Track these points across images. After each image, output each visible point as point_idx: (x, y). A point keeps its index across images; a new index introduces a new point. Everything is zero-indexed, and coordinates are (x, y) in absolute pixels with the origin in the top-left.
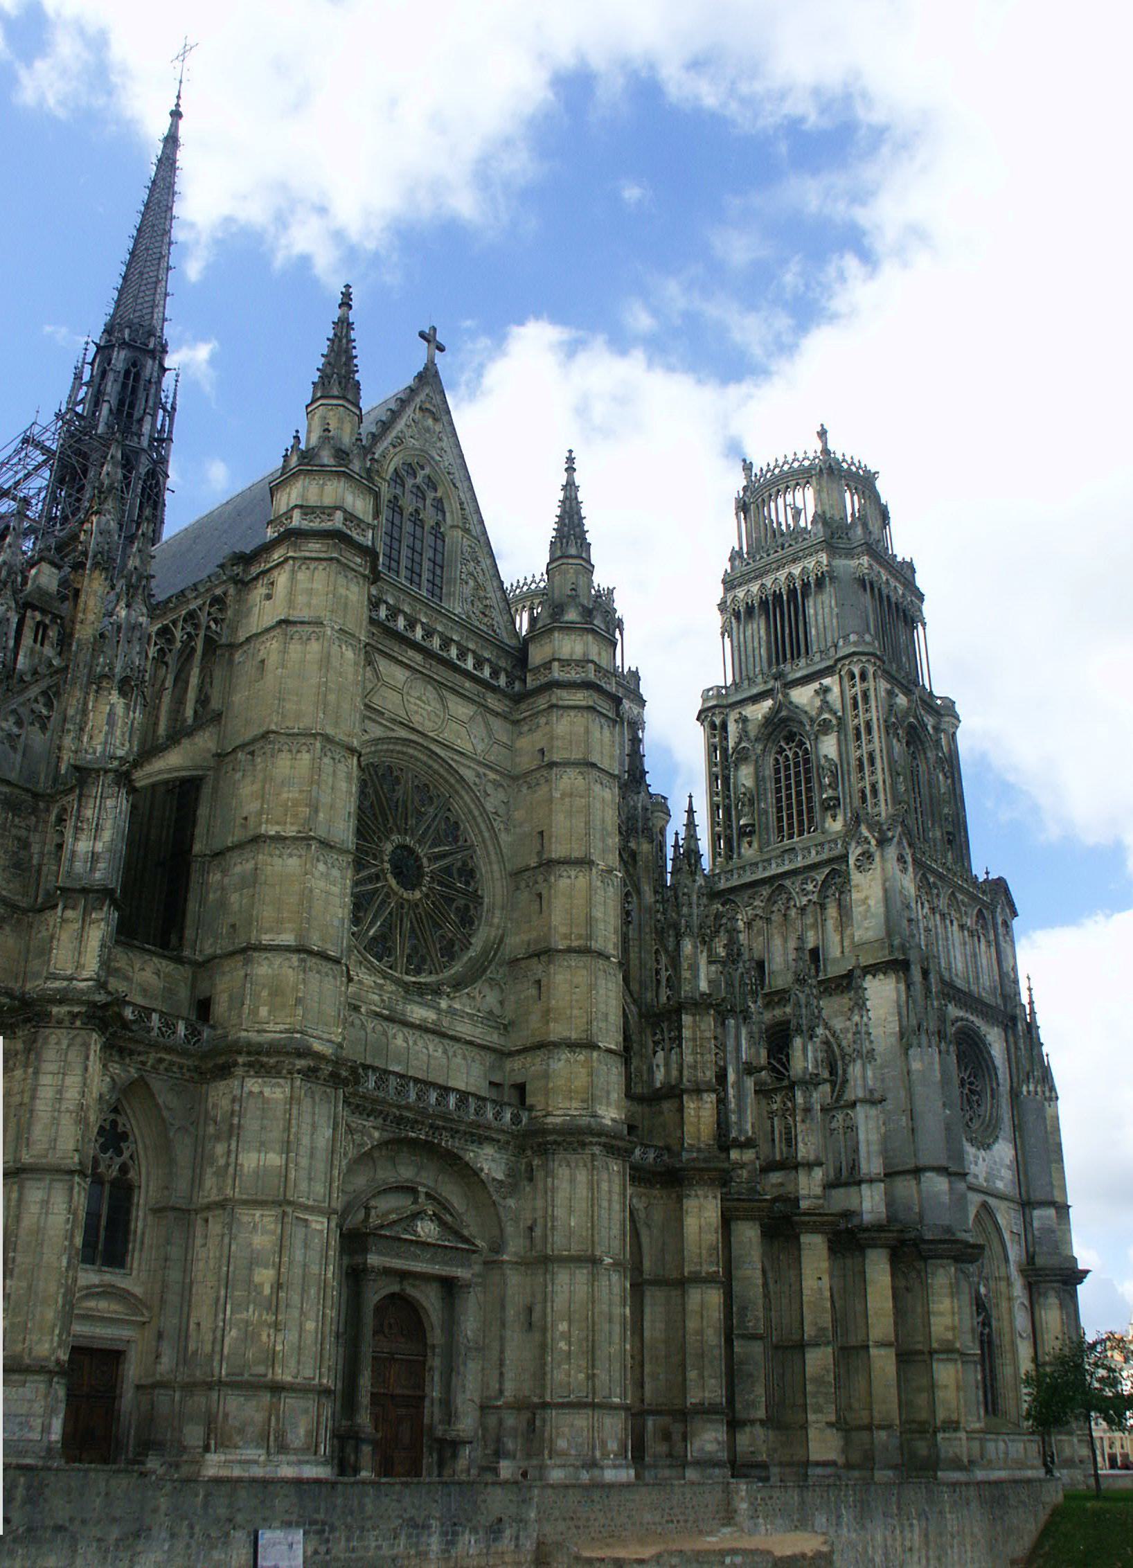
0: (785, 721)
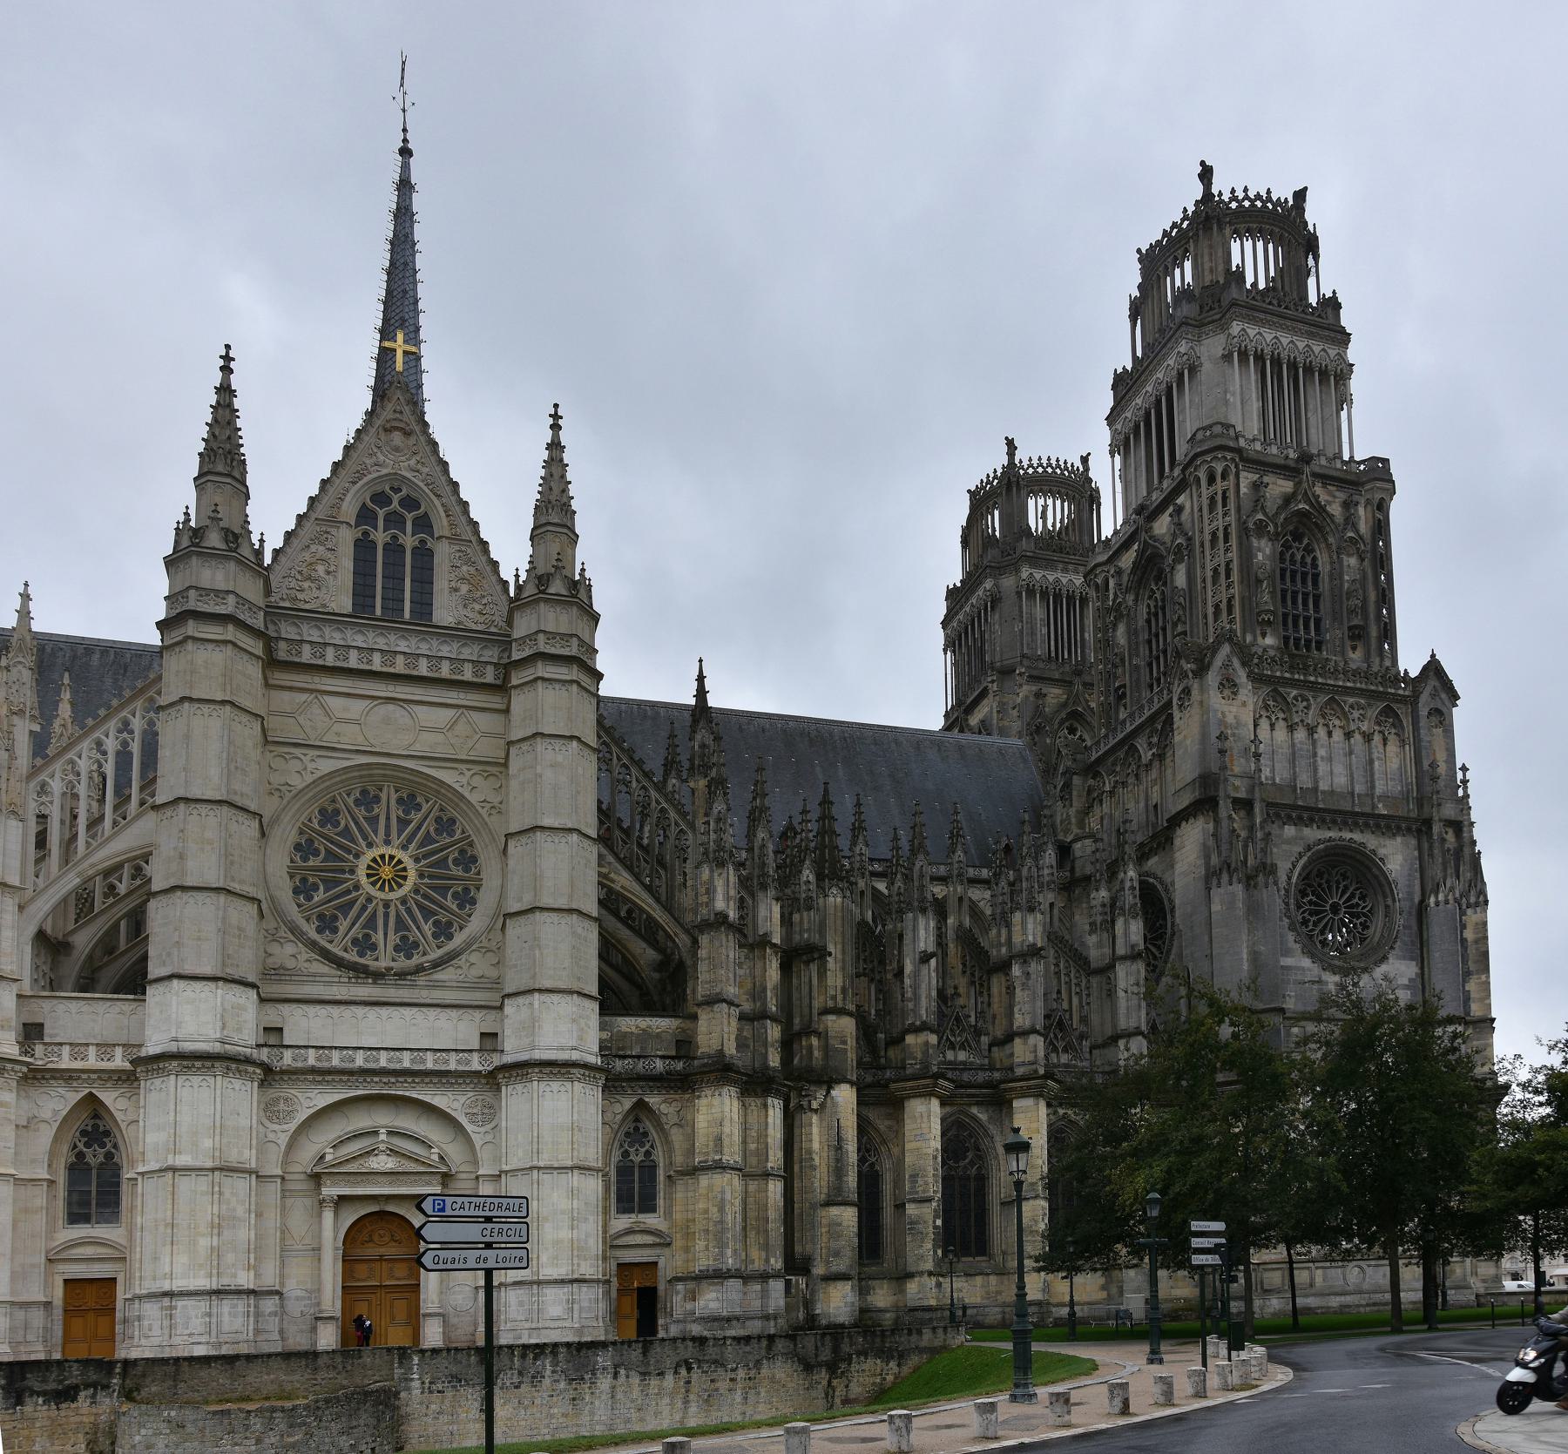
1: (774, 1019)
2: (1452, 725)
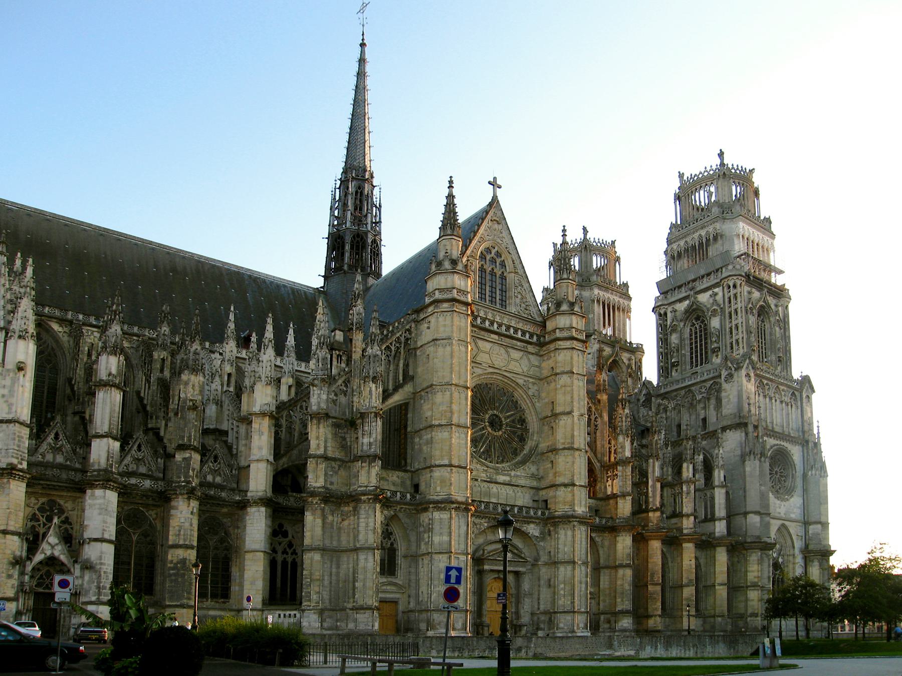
0: (694, 310)
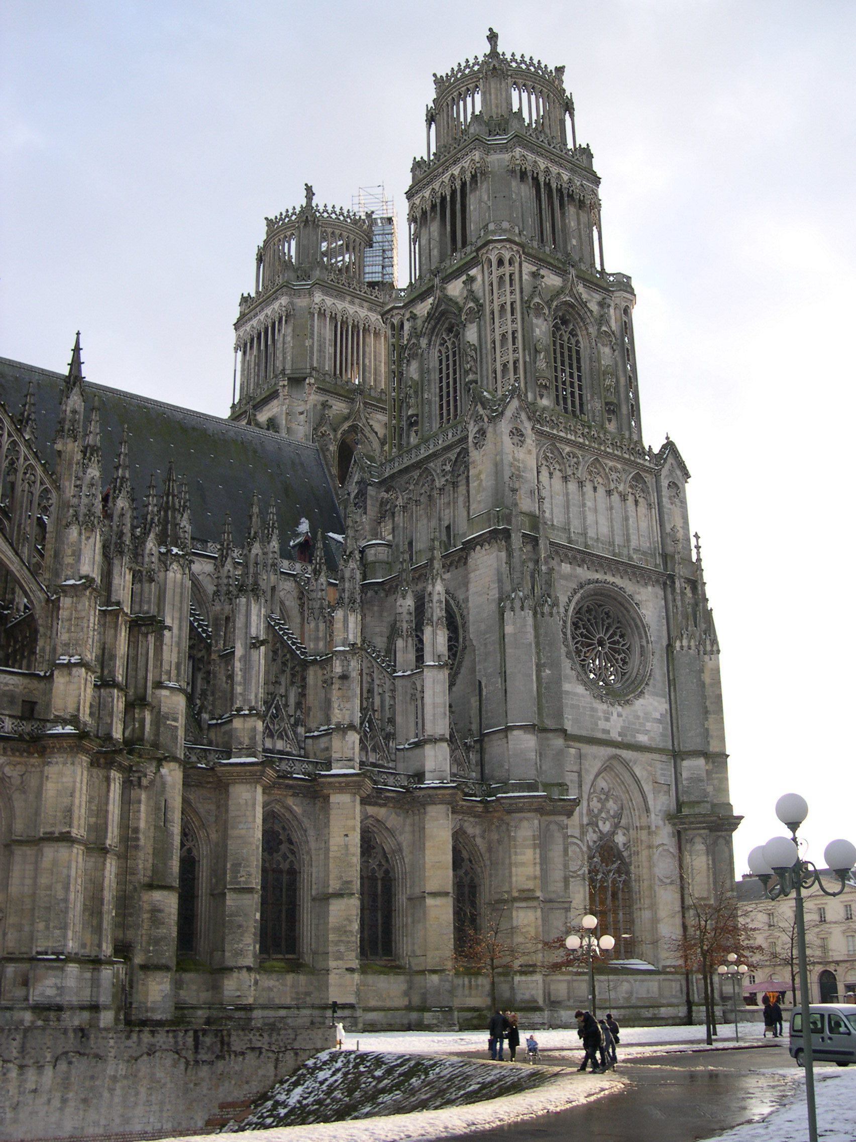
0: (443, 314)
1: (120, 689)
2: (685, 498)
